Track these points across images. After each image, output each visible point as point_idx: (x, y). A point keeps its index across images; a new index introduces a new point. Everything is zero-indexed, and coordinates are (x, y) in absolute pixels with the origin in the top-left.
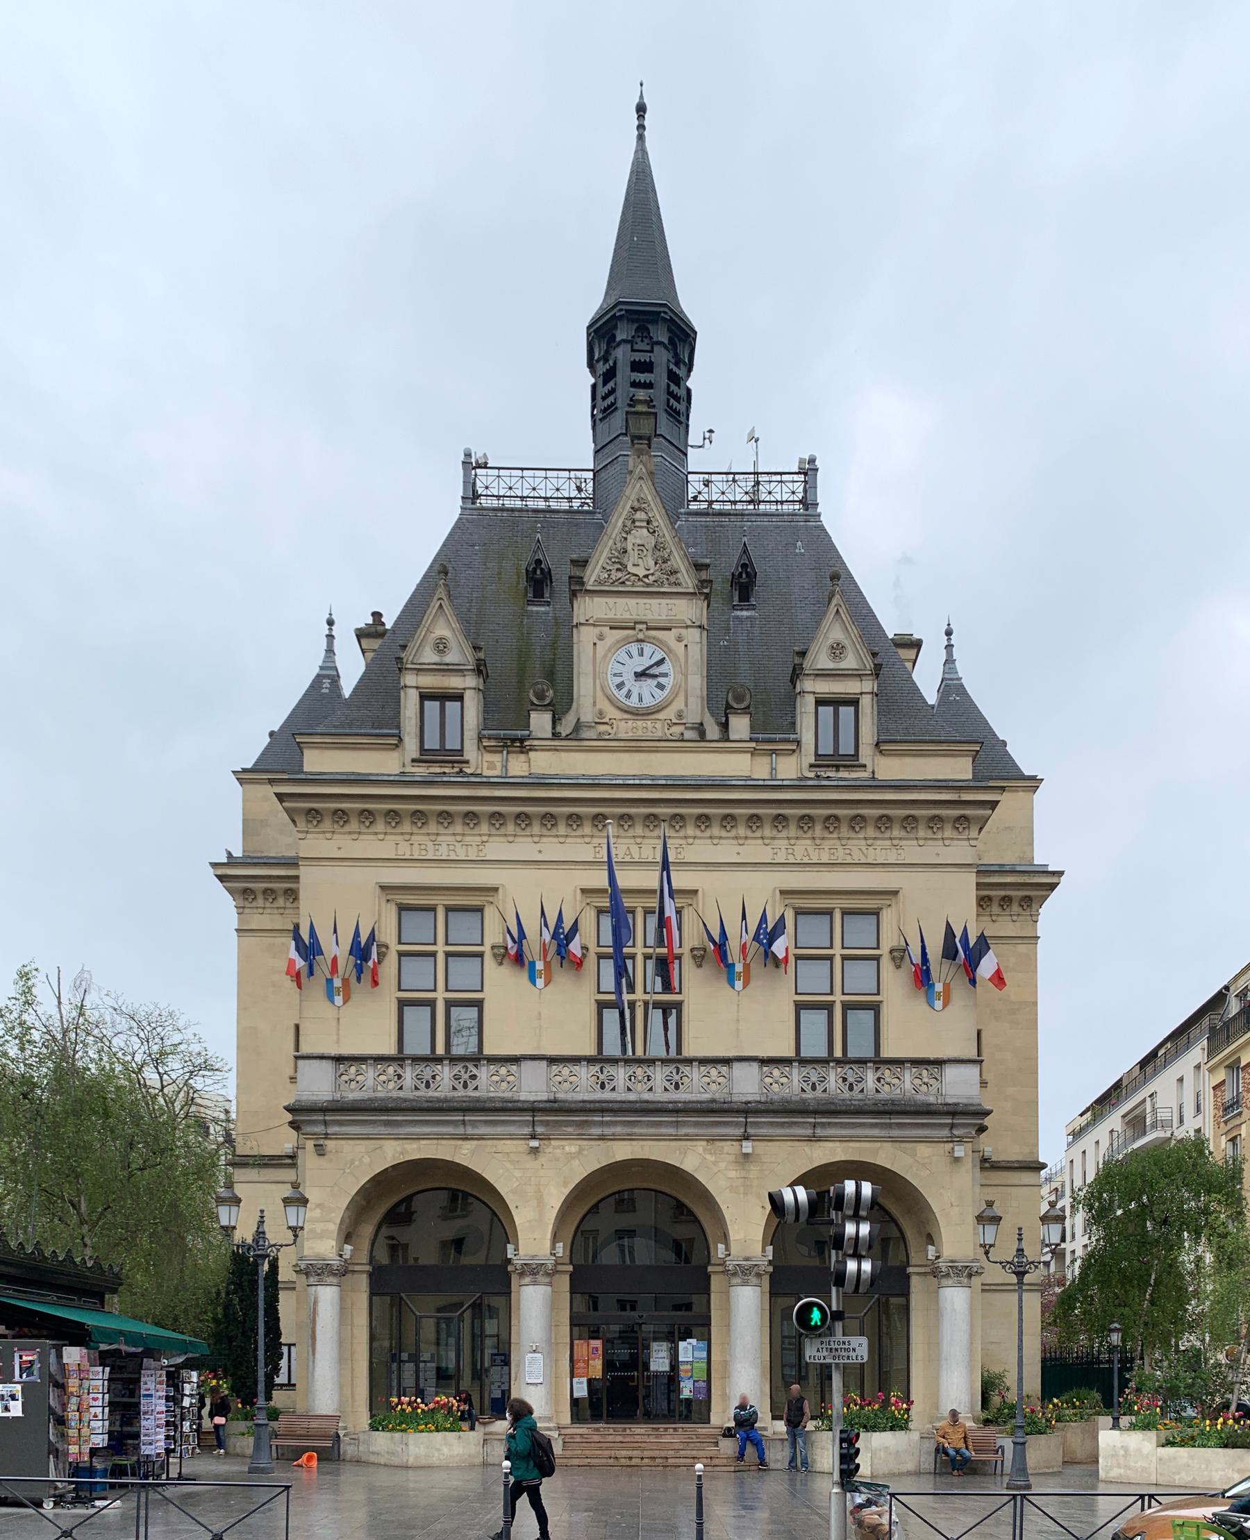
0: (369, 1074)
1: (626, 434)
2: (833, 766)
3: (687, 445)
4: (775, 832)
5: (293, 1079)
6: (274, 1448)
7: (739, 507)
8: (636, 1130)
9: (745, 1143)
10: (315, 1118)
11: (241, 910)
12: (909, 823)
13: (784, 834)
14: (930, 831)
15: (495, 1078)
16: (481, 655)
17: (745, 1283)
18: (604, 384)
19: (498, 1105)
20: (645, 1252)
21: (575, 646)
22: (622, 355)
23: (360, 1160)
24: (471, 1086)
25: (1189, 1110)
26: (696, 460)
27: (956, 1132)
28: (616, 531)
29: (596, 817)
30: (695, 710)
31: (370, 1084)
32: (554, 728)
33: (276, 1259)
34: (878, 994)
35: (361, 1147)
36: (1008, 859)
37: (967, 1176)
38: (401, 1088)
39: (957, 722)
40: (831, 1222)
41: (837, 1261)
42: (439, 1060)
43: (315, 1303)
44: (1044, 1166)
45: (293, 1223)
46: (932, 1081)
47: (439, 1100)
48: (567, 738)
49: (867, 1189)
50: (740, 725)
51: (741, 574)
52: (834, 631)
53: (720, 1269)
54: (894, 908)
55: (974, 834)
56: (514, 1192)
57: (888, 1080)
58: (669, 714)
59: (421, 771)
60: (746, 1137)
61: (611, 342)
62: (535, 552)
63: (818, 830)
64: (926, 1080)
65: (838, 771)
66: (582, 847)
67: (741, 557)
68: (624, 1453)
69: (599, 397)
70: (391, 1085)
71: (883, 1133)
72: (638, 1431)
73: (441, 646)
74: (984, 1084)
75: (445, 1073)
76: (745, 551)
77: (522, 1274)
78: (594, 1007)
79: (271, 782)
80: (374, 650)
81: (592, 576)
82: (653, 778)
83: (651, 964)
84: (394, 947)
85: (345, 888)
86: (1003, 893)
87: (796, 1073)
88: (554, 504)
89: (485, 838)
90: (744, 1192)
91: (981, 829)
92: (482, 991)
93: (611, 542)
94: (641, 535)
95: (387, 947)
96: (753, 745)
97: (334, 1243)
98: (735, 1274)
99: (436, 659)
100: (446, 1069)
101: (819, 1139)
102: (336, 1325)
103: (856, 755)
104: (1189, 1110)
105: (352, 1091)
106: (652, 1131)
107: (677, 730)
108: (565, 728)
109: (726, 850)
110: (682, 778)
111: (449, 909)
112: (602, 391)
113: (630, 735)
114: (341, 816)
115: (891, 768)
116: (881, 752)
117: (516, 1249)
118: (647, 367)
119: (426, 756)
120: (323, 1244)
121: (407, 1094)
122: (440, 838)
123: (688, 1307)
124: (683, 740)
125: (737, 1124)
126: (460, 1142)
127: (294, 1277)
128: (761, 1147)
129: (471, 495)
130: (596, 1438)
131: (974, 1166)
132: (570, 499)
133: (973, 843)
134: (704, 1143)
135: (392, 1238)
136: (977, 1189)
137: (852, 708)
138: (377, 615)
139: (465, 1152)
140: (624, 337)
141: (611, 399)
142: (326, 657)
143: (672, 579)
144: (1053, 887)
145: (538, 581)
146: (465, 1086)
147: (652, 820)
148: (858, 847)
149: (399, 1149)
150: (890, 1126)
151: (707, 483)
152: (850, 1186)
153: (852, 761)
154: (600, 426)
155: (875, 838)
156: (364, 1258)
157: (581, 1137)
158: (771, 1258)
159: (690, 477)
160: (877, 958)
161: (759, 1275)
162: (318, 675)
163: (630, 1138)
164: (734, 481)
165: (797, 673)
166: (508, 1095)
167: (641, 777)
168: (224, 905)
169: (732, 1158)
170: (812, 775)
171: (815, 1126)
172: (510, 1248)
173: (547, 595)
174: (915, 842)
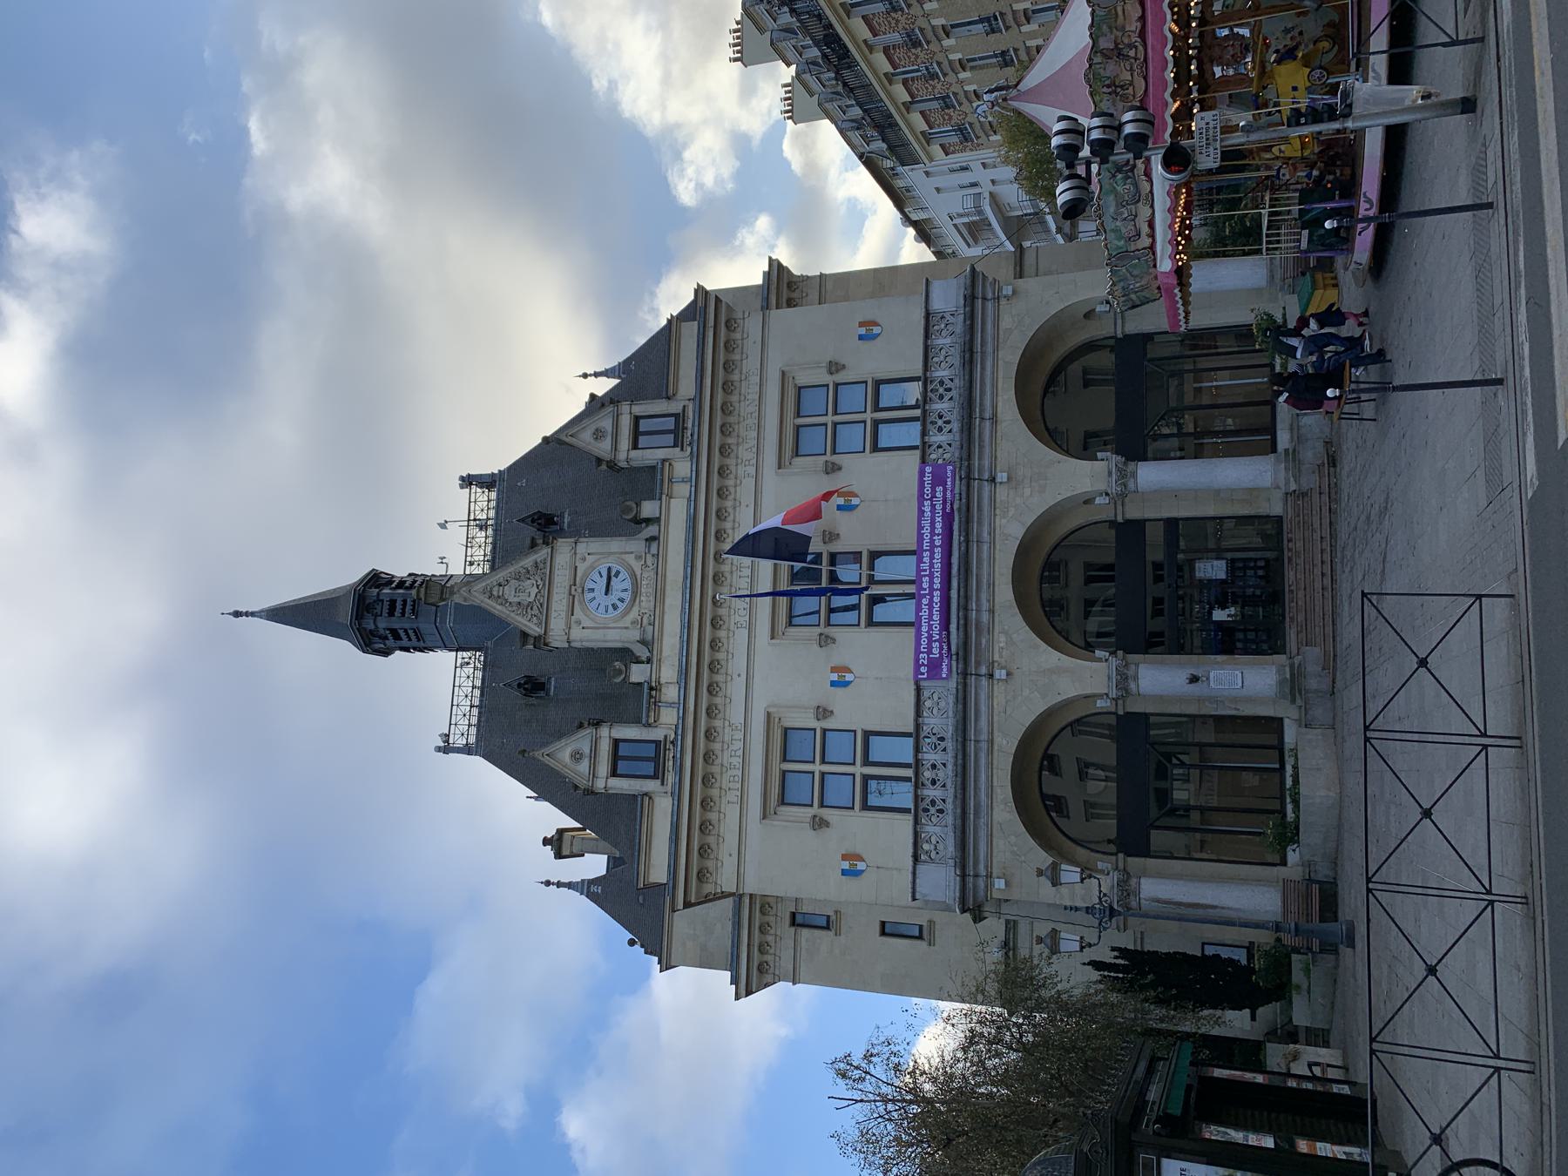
9: (998, 480)
13: (733, 468)
27: (990, 296)
30: (637, 545)
31: (940, 831)
35: (999, 843)
37: (1029, 284)
47: (955, 764)
48: (651, 651)
50: (648, 509)
59: (671, 778)
60: (993, 480)
68: (1318, 585)
75: (930, 757)
82: (685, 578)
90: (1043, 483)
100: (926, 756)
103: (676, 415)
106: (985, 564)
108: (643, 653)
114: (704, 851)
153: (679, 418)
160: (837, 385)
163: (992, 585)
165: (612, 465)
166: (951, 700)
171: (982, 419)
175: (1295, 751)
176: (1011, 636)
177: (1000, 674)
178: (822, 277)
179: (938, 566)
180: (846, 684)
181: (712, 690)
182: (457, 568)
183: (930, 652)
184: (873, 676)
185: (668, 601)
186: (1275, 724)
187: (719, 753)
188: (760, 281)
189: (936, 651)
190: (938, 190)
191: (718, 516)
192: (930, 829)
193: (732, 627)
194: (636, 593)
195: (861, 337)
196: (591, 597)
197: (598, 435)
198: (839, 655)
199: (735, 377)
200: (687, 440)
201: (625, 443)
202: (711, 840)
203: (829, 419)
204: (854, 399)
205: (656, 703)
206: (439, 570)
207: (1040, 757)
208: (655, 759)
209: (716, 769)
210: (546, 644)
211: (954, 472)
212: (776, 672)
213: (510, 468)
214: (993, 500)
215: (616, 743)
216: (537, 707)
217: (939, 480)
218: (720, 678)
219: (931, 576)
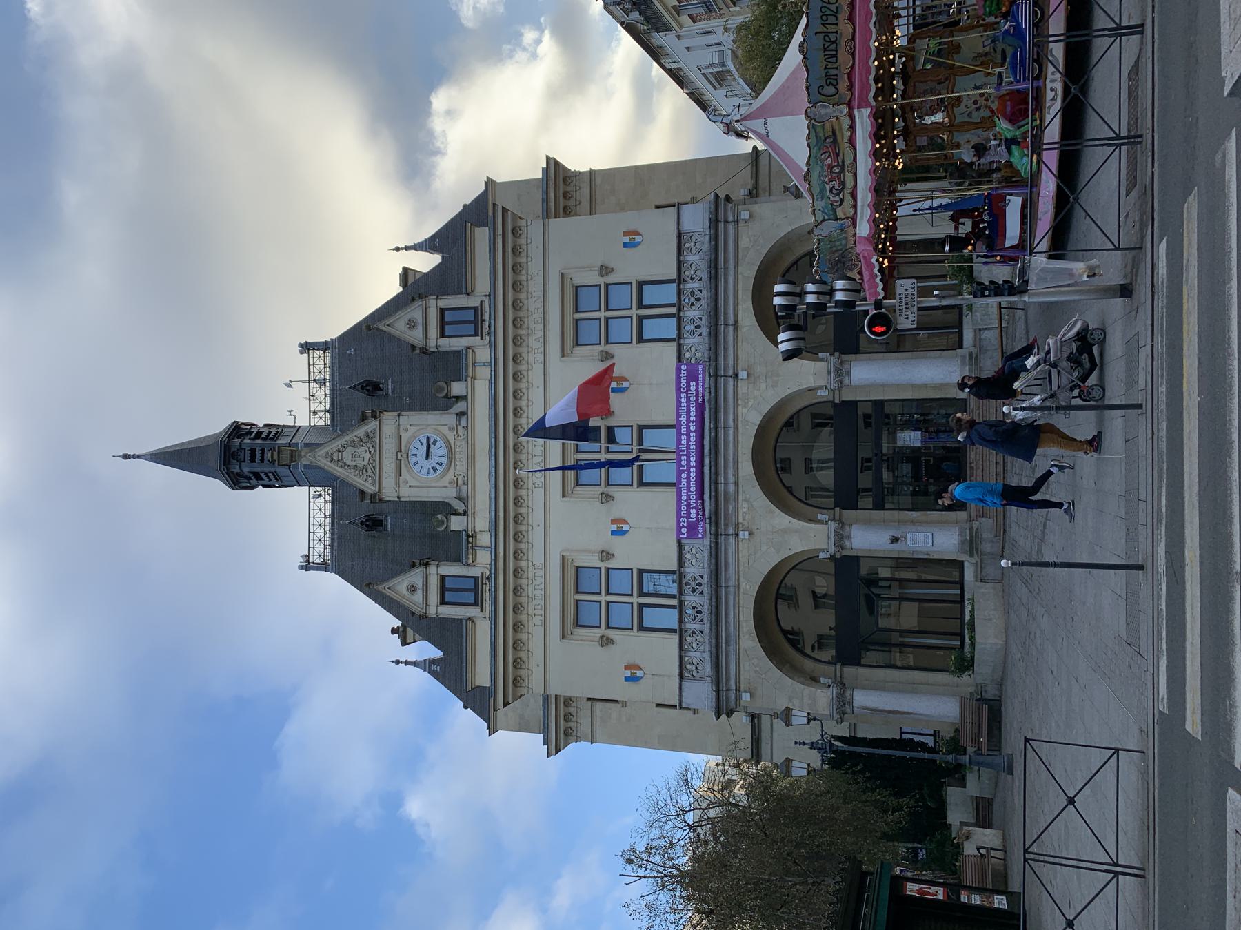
0: (693, 655)
5: (695, 712)
7: (328, 392)
11: (578, 739)
12: (516, 269)
13: (524, 355)
17: (849, 373)
22: (246, 470)
24: (699, 580)
25: (711, 39)
27: (730, 219)
29: (516, 486)
30: (449, 418)
31: (700, 655)
33: (833, 737)
35: (745, 665)
36: (538, 196)
42: (681, 602)
43: (867, 709)
44: (755, 148)
45: (805, 721)
46: (693, 239)
47: (710, 605)
48: (466, 506)
50: (457, 388)
53: (837, 393)
55: (523, 223)
59: (488, 606)
66: (534, 499)
70: (700, 639)
71: (731, 273)
72: (973, 457)
74: (694, 201)
75: (690, 599)
76: (354, 387)
77: (843, 548)
78: (642, 489)
79: (495, 710)
82: (491, 447)
84: (602, 631)
85: (566, 662)
87: (689, 341)
88: (329, 513)
90: (774, 377)
99: (420, 592)
100: (687, 598)
101: (736, 321)
102: (884, 694)
103: (475, 308)
104: (711, 39)
107: (461, 431)
108: (460, 507)
110: (490, 426)
111: (577, 591)
112: (266, 482)
114: (517, 663)
115: (482, 284)
118: (253, 451)
119: (478, 602)
120: (822, 699)
123: (867, 416)
127: (846, 724)
128: (742, 363)
132: (326, 502)
138: (394, 631)
144: (556, 163)
145: (373, 523)
146: (700, 584)
147: (516, 448)
150: (726, 269)
151: (315, 413)
153: (478, 311)
156: (832, 668)
157: (736, 500)
160: (607, 285)
161: (842, 363)
165: (425, 351)
166: (706, 553)
167: (490, 456)
169: (751, 386)
172: (822, 556)
173: (381, 518)
175: (972, 599)
176: (751, 502)
177: (744, 535)
178: (592, 173)
179: (693, 447)
180: (624, 533)
181: (517, 537)
182: (303, 421)
183: (688, 516)
184: (645, 527)
186: (960, 565)
188: (540, 176)
189: (693, 516)
190: (688, 49)
191: (515, 397)
192: (692, 654)
194: (451, 459)
195: (625, 245)
196: (416, 459)
197: (411, 324)
198: (617, 510)
199: (523, 277)
200: (485, 331)
202: (522, 654)
203: (602, 314)
204: (622, 297)
205: (473, 548)
206: (289, 422)
207: (777, 591)
208: (475, 591)
209: (523, 600)
210: (380, 500)
211: (704, 371)
213: (340, 338)
214: (736, 393)
215: (443, 578)
216: (377, 541)
217: (692, 376)
218: (523, 528)
219: (688, 455)
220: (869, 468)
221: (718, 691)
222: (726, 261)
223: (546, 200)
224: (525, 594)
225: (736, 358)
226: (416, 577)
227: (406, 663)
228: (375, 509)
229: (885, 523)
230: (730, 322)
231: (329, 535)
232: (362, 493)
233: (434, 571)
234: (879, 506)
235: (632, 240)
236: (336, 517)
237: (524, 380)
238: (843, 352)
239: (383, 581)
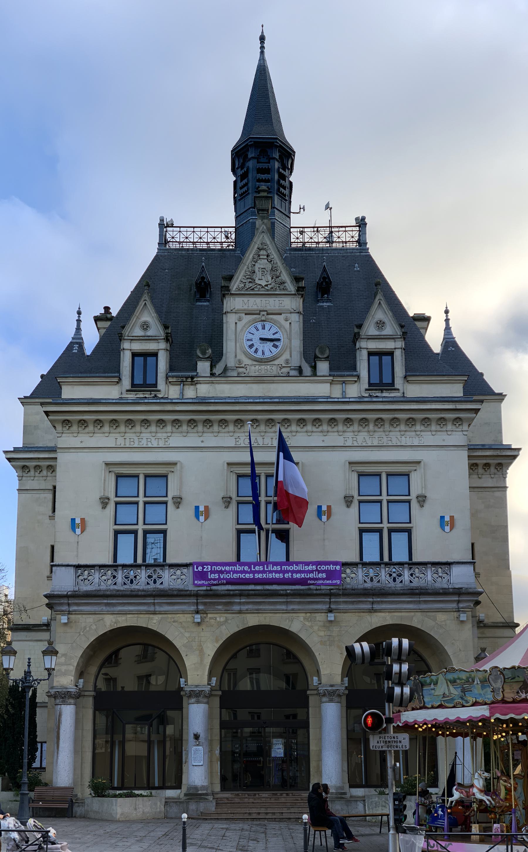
0: (96, 576)
1: (254, 208)
2: (379, 390)
3: (290, 212)
4: (345, 428)
5: (49, 578)
6: (31, 809)
7: (321, 245)
8: (261, 607)
9: (329, 615)
10: (62, 601)
11: (20, 478)
12: (426, 421)
13: (351, 429)
14: (438, 427)
15: (173, 577)
16: (169, 331)
17: (331, 701)
18: (241, 182)
19: (175, 593)
20: (269, 683)
21: (225, 325)
22: (251, 164)
23: (90, 627)
24: (159, 582)
26: (295, 220)
27: (461, 605)
28: (249, 261)
30: (296, 360)
31: (97, 581)
32: (211, 370)
34: (410, 522)
35: (90, 619)
36: (488, 441)
38: (115, 584)
39: (453, 360)
40: (384, 663)
41: (388, 687)
42: (139, 566)
43: (60, 715)
44: (517, 625)
45: (48, 666)
47: (139, 590)
48: (219, 376)
49: (406, 642)
50: (323, 367)
51: (322, 283)
52: (379, 313)
53: (315, 692)
54: (418, 471)
55: (465, 427)
56: (184, 646)
57: (417, 575)
58: (281, 361)
59: (132, 396)
60: (330, 611)
61: (246, 159)
62: (201, 273)
63: (371, 427)
64: (440, 575)
65: (382, 392)
66: (226, 438)
67: (322, 273)
68: (254, 810)
69: (238, 187)
70: (110, 582)
72: (264, 795)
73: (145, 326)
74: (477, 575)
75: (143, 574)
77: (190, 697)
78: (235, 533)
79: (42, 404)
80: (104, 328)
81: (235, 285)
82: (271, 398)
83: (270, 507)
84: (113, 499)
85: (85, 466)
86: (485, 462)
88: (212, 246)
89: (169, 434)
91: (469, 425)
92: (166, 524)
93: (246, 267)
94: (263, 263)
95: (109, 499)
96: (331, 378)
97: (73, 678)
98: (324, 695)
100: (143, 572)
101: (376, 611)
102: (73, 729)
103: (393, 384)
105: (87, 586)
107: (285, 370)
108: (218, 370)
109: (316, 440)
111: (147, 476)
112: (240, 184)
113: (257, 374)
114: (83, 423)
116: (408, 381)
117: (186, 681)
118: (267, 171)
119: (134, 387)
120: (66, 680)
121: (119, 587)
122: (142, 435)
123: (295, 716)
124: (289, 376)
125: (324, 603)
126: (151, 616)
127: (46, 699)
129: (163, 242)
130: (237, 800)
131: (473, 626)
132: (221, 243)
133: (465, 433)
134: (303, 615)
135: (106, 674)
136: (476, 640)
137: (390, 357)
138: (107, 309)
139: (155, 621)
140: (253, 155)
141: (245, 189)
142: (76, 332)
143: (282, 287)
144: (515, 457)
145: (202, 289)
146: (155, 582)
147: (270, 422)
148: (395, 436)
149: (114, 620)
150: (419, 602)
151: (302, 233)
152: (395, 641)
153: (391, 386)
154: (238, 203)
155: (406, 431)
156: (91, 688)
157: (227, 611)
158: (347, 685)
159: (292, 230)
160: (409, 502)
161: (339, 696)
162: (71, 342)
163: (258, 612)
164: (317, 231)
165: (356, 337)
166: (181, 587)
168: (11, 474)
169: (321, 624)
170: (367, 395)
171: (373, 603)
172: (182, 680)
174: (430, 433)
175: (151, 796)
176: (225, 624)
177: (198, 618)
179: (270, 576)
183: (212, 572)
184: (202, 534)
185: (255, 386)
187: (149, 430)
189: (212, 576)
192: (97, 575)
193: (237, 435)
199: (418, 427)
200: (374, 393)
201: (373, 345)
202: (91, 428)
204: (399, 514)
207: (152, 645)
211: (335, 585)
212: (202, 466)
215: (155, 355)
217: (331, 575)
218: (200, 428)
219: (264, 572)
220: (253, 718)
221: (67, 596)
222: (425, 602)
223: (483, 448)
224: (143, 430)
225: (346, 611)
226: (156, 329)
227: (79, 321)
228: (216, 291)
229: (209, 729)
230: (376, 606)
231: (191, 246)
232: (230, 278)
233: (160, 346)
234: (223, 725)
235: (446, 523)
236: (207, 253)
237: (330, 429)
238: (349, 698)
239: (152, 299)
